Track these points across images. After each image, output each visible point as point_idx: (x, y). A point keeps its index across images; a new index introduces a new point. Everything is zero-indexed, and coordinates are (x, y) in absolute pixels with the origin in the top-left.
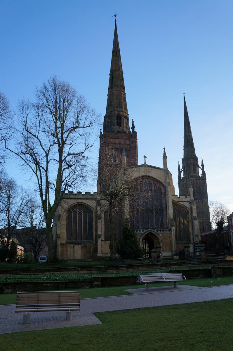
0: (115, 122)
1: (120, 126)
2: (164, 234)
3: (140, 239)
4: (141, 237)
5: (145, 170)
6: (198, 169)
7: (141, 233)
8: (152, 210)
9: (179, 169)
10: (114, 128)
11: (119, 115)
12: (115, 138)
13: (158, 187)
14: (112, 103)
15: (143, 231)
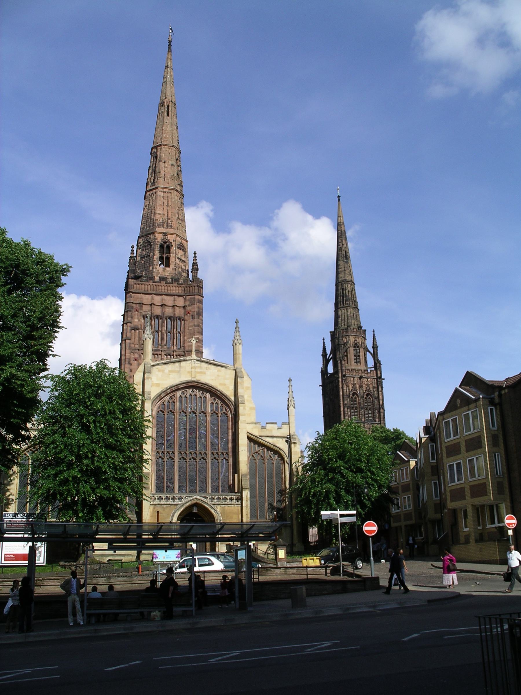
2: (226, 507)
3: (173, 516)
4: (174, 513)
6: (365, 355)
7: (176, 505)
9: (324, 354)
10: (153, 270)
11: (165, 242)
12: (154, 292)
15: (180, 499)
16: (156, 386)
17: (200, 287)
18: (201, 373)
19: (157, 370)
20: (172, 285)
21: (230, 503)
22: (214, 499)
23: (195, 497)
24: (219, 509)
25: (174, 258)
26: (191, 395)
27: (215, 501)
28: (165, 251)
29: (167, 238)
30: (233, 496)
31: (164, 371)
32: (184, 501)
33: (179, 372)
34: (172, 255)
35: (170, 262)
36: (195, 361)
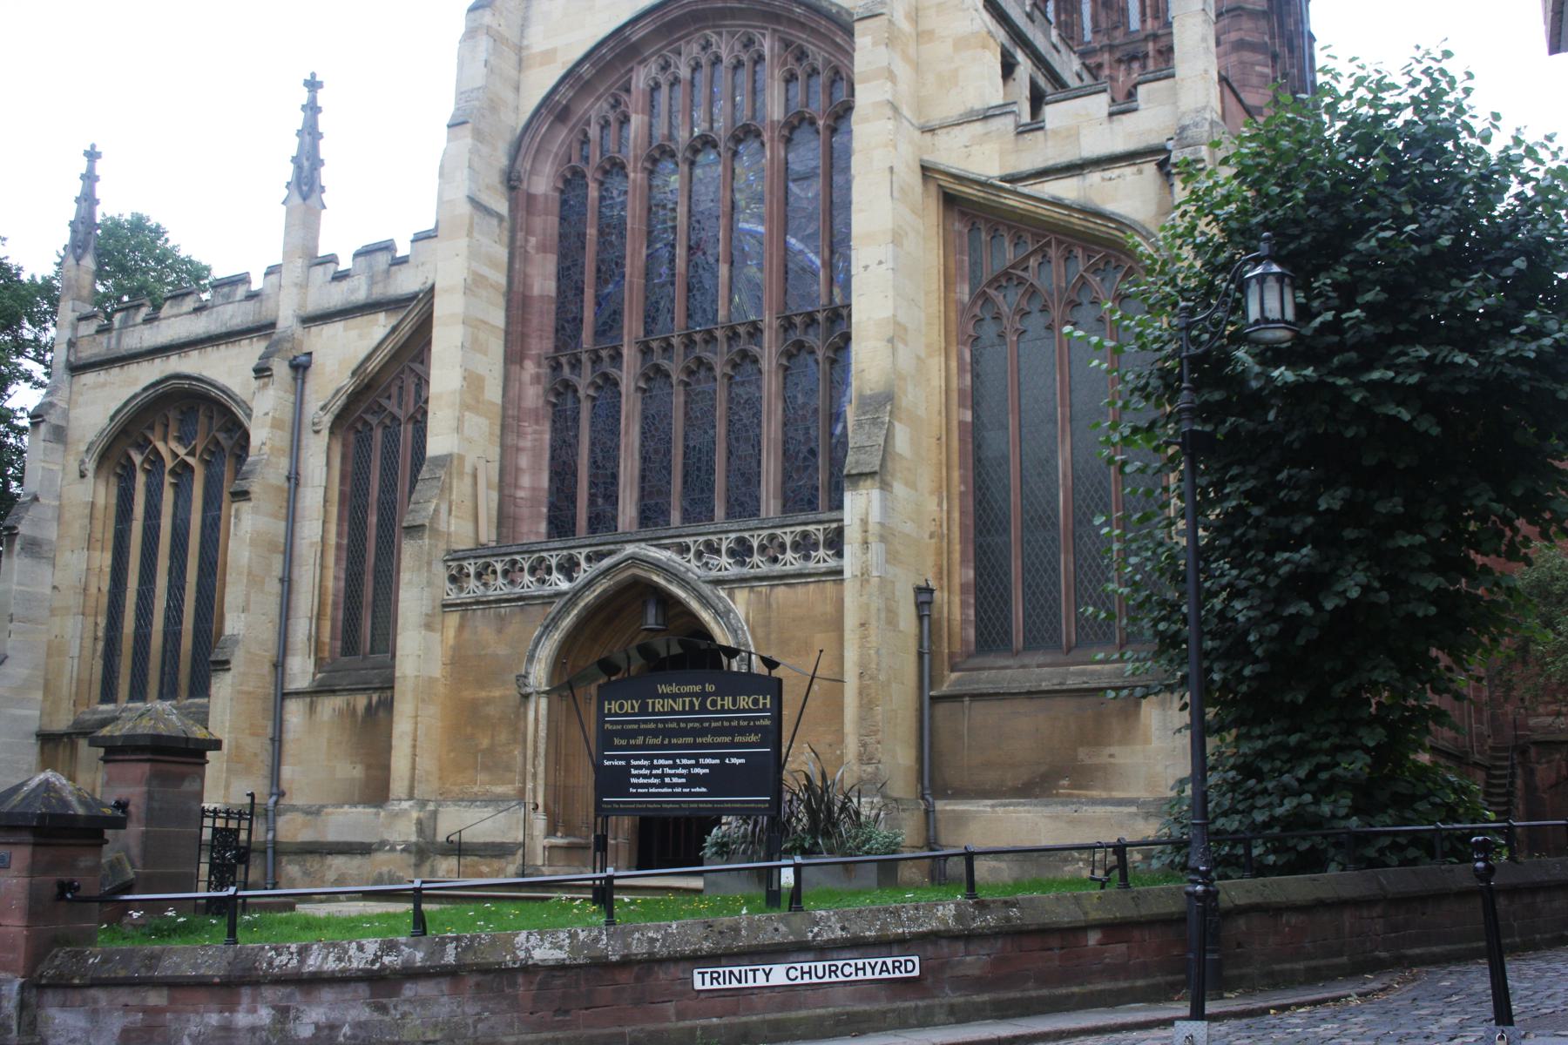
2: (781, 592)
3: (531, 658)
7: (549, 599)
8: (755, 331)
15: (569, 568)
16: (542, 64)
22: (718, 552)
23: (630, 549)
24: (741, 604)
26: (696, 67)
27: (725, 565)
30: (811, 528)
32: (581, 577)
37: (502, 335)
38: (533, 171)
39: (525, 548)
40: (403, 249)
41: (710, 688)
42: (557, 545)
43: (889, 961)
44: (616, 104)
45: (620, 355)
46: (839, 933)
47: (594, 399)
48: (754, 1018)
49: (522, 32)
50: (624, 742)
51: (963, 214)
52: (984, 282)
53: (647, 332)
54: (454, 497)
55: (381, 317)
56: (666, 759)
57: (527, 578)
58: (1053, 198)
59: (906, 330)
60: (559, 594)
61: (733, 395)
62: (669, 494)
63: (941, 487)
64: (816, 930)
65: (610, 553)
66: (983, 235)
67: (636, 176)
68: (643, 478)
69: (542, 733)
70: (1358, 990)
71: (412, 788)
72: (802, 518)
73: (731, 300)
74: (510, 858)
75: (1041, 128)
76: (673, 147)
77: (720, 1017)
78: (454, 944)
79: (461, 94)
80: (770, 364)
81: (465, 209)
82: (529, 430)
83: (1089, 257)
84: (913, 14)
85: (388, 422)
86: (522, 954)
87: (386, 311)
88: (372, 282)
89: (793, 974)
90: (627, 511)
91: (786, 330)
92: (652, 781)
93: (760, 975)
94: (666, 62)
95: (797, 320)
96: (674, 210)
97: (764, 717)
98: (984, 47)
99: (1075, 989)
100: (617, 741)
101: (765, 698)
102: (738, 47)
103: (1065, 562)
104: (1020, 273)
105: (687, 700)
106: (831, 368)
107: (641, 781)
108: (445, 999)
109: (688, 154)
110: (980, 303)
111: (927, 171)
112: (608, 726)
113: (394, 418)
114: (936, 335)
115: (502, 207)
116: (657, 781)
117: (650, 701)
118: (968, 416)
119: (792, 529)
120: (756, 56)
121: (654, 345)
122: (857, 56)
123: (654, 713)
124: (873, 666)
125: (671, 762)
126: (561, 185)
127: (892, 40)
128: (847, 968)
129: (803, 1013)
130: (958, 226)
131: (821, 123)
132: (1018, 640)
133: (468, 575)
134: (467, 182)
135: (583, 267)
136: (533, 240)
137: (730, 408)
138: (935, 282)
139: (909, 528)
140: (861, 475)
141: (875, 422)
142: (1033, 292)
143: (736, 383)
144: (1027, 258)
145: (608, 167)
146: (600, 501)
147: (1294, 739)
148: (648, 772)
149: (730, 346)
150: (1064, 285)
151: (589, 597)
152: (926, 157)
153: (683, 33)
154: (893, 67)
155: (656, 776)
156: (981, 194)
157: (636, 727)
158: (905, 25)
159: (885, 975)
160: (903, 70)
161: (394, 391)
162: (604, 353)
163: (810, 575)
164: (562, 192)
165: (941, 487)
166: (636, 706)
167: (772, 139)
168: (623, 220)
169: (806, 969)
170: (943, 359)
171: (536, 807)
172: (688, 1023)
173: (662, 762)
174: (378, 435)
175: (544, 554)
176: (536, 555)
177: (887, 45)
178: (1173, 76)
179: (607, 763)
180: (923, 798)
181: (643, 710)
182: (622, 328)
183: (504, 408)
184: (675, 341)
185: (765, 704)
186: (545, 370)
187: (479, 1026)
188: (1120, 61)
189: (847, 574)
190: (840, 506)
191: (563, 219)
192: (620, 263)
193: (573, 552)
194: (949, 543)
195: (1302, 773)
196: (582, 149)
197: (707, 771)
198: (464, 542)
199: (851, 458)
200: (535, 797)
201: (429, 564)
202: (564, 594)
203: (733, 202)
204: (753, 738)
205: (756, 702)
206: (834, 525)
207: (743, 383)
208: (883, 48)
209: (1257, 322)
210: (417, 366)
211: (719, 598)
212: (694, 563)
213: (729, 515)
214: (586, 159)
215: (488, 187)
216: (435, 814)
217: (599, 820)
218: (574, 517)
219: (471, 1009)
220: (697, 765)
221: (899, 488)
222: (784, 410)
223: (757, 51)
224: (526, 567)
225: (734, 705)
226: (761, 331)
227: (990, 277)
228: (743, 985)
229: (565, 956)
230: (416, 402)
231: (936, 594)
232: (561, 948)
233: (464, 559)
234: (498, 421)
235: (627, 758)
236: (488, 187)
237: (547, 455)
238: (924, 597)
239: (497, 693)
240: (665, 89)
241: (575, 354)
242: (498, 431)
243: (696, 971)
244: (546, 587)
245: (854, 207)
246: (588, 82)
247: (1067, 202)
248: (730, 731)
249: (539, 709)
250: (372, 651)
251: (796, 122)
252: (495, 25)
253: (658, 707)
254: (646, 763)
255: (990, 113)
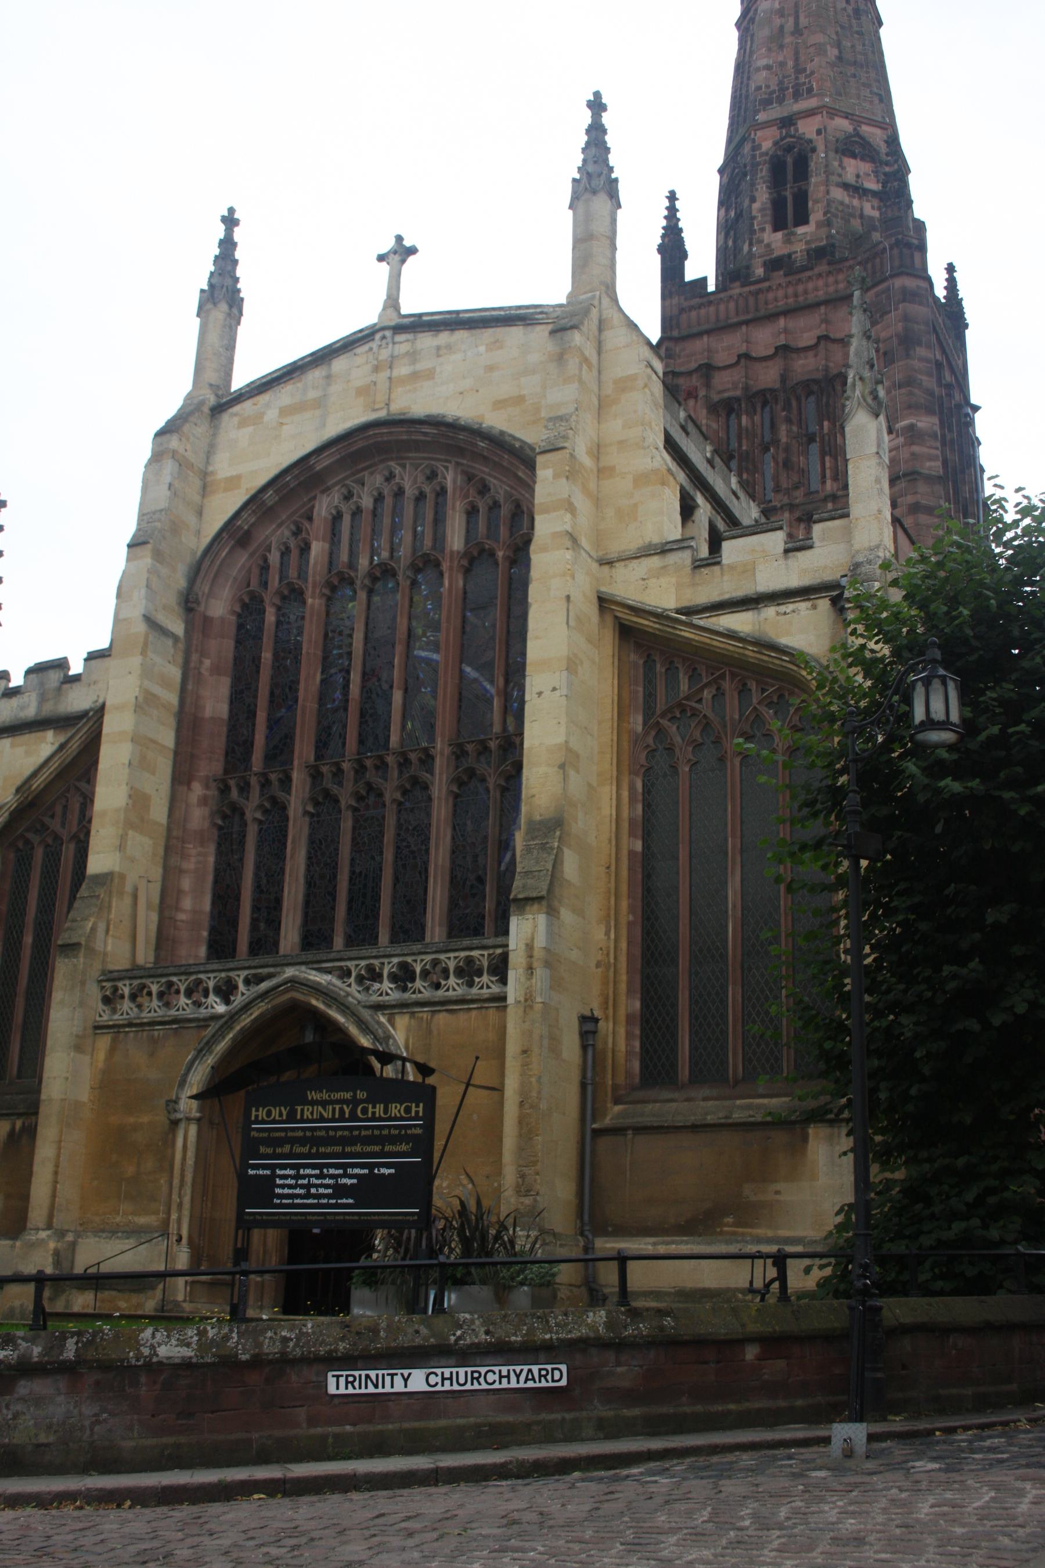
0: (756, 206)
1: (802, 218)
2: (442, 1018)
5: (376, 369)
8: (427, 759)
10: (750, 250)
11: (789, 149)
13: (505, 511)
14: (747, 91)
15: (226, 991)
16: (226, 490)
17: (909, 245)
18: (415, 376)
19: (236, 420)
20: (809, 273)
21: (460, 991)
23: (290, 972)
25: (822, 188)
26: (379, 499)
27: (387, 990)
28: (790, 176)
29: (797, 130)
30: (475, 953)
31: (261, 415)
32: (238, 1000)
33: (319, 403)
34: (813, 180)
35: (810, 204)
36: (388, 333)
37: (171, 756)
38: (211, 594)
39: (183, 969)
40: (76, 667)
41: (361, 1095)
42: (215, 967)
43: (535, 1369)
44: (297, 532)
45: (289, 779)
46: (483, 1337)
47: (260, 822)
48: (390, 1427)
49: (208, 458)
50: (270, 1151)
51: (638, 646)
52: (658, 712)
53: (319, 757)
54: (112, 916)
55: (50, 734)
56: (313, 1169)
57: (183, 1000)
58: (729, 630)
59: (578, 756)
60: (216, 1017)
61: (402, 821)
62: (332, 920)
63: (608, 915)
64: (459, 1333)
65: (270, 976)
66: (658, 666)
67: (314, 602)
68: (307, 903)
69: (190, 1161)
70: (1027, 1416)
71: (51, 1216)
72: (466, 942)
73: (404, 727)
74: (150, 1293)
75: (719, 563)
76: (352, 574)
77: (354, 1424)
78: (75, 1339)
79: (142, 516)
80: (440, 790)
81: (141, 627)
82: (193, 852)
83: (763, 690)
84: (596, 452)
85: (50, 841)
86: (146, 1351)
87: (55, 729)
88: (43, 699)
89: (433, 1379)
90: (290, 936)
91: (458, 758)
92: (298, 1191)
93: (399, 1381)
94: (350, 492)
95: (469, 748)
96: (351, 636)
97: (415, 1126)
98: (663, 484)
99: (732, 1407)
100: (262, 1150)
101: (417, 1106)
102: (421, 478)
103: (733, 994)
104: (694, 705)
105: (337, 1107)
106: (502, 796)
107: (286, 1191)
108: (60, 1399)
109: (367, 582)
110: (653, 733)
111: (604, 602)
112: (254, 1134)
113: (57, 837)
114: (608, 764)
115: (178, 628)
116: (302, 1191)
117: (299, 1108)
118: (638, 846)
119: (456, 954)
120: (438, 488)
121: (325, 769)
122: (538, 488)
123: (302, 1121)
124: (534, 1094)
125: (317, 1172)
126: (238, 609)
127: (572, 473)
128: (490, 1375)
129: (443, 1423)
130: (633, 657)
131: (500, 554)
132: (684, 1072)
133: (122, 997)
134: (144, 601)
135: (257, 690)
136: (207, 663)
137: (399, 835)
138: (608, 711)
139: (575, 955)
140: (527, 900)
141: (544, 847)
142: (707, 726)
143: (406, 809)
144: (702, 689)
145: (286, 592)
146: (262, 926)
147: (961, 1162)
148: (293, 1182)
149: (401, 772)
150: (737, 717)
151: (246, 1020)
152: (603, 589)
153: (368, 463)
154: (573, 500)
155: (302, 1186)
156: (657, 626)
157: (283, 1134)
158: (587, 462)
159: (530, 1384)
160: (581, 503)
161: (59, 809)
162: (273, 777)
163: (473, 1001)
164: (239, 616)
165: (608, 915)
166: (285, 1113)
167: (451, 568)
168: (298, 646)
169: (447, 1375)
170: (614, 788)
171: (179, 1240)
172: (319, 1430)
173: (308, 1171)
174: (39, 853)
175: (202, 976)
176: (193, 977)
177: (567, 478)
178: (847, 515)
179: (251, 1172)
180: (582, 1234)
181: (291, 1118)
182: (292, 752)
183: (169, 829)
184: (345, 766)
185: (417, 1112)
186: (213, 792)
187: (97, 1428)
188: (799, 520)
189: (510, 1000)
190: (506, 933)
191: (238, 642)
192: (293, 686)
193: (232, 974)
194: (616, 972)
195: (970, 1196)
196: (261, 575)
197: (355, 1181)
198: (120, 961)
199: (517, 883)
200: (179, 1228)
201: (83, 983)
202: (220, 1016)
203: (409, 630)
204: (404, 1147)
205: (408, 1110)
206: (499, 951)
207: (412, 810)
208: (564, 480)
209: (922, 723)
210: (83, 785)
211: (379, 1023)
212: (354, 989)
213: (394, 940)
214: (265, 585)
215: (164, 607)
216: (73, 1245)
217: (240, 1232)
218: (235, 942)
219: (89, 1410)
220: (345, 1175)
221: (566, 915)
222: (453, 838)
223: (440, 483)
224: (182, 989)
225: (386, 1111)
226: (432, 758)
227: (664, 708)
228: (380, 1390)
229: (193, 1354)
230: (80, 822)
231: (601, 1024)
232: (188, 1345)
233: (120, 979)
234: (162, 842)
235: (273, 1167)
236: (164, 607)
237: (210, 878)
238: (590, 1026)
239: (145, 1119)
240: (347, 519)
241: (243, 777)
242: (161, 851)
243: (330, 1374)
244: (202, 1010)
245: (530, 635)
246: (271, 509)
247: (742, 635)
248: (381, 1140)
249: (187, 1138)
250: (19, 1076)
251: (475, 554)
252: (181, 451)
253: (307, 1114)
254: (292, 1172)
255: (668, 547)
